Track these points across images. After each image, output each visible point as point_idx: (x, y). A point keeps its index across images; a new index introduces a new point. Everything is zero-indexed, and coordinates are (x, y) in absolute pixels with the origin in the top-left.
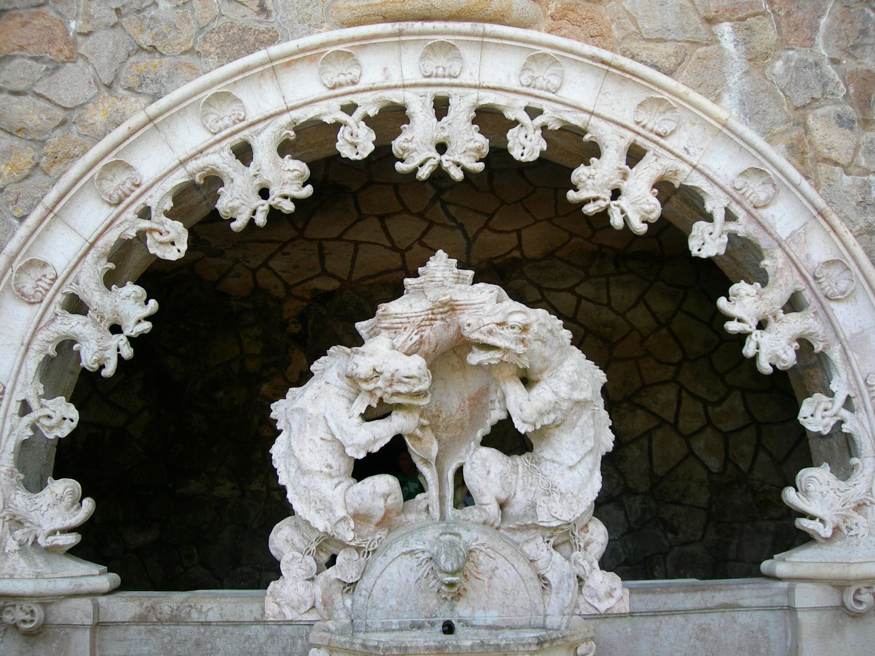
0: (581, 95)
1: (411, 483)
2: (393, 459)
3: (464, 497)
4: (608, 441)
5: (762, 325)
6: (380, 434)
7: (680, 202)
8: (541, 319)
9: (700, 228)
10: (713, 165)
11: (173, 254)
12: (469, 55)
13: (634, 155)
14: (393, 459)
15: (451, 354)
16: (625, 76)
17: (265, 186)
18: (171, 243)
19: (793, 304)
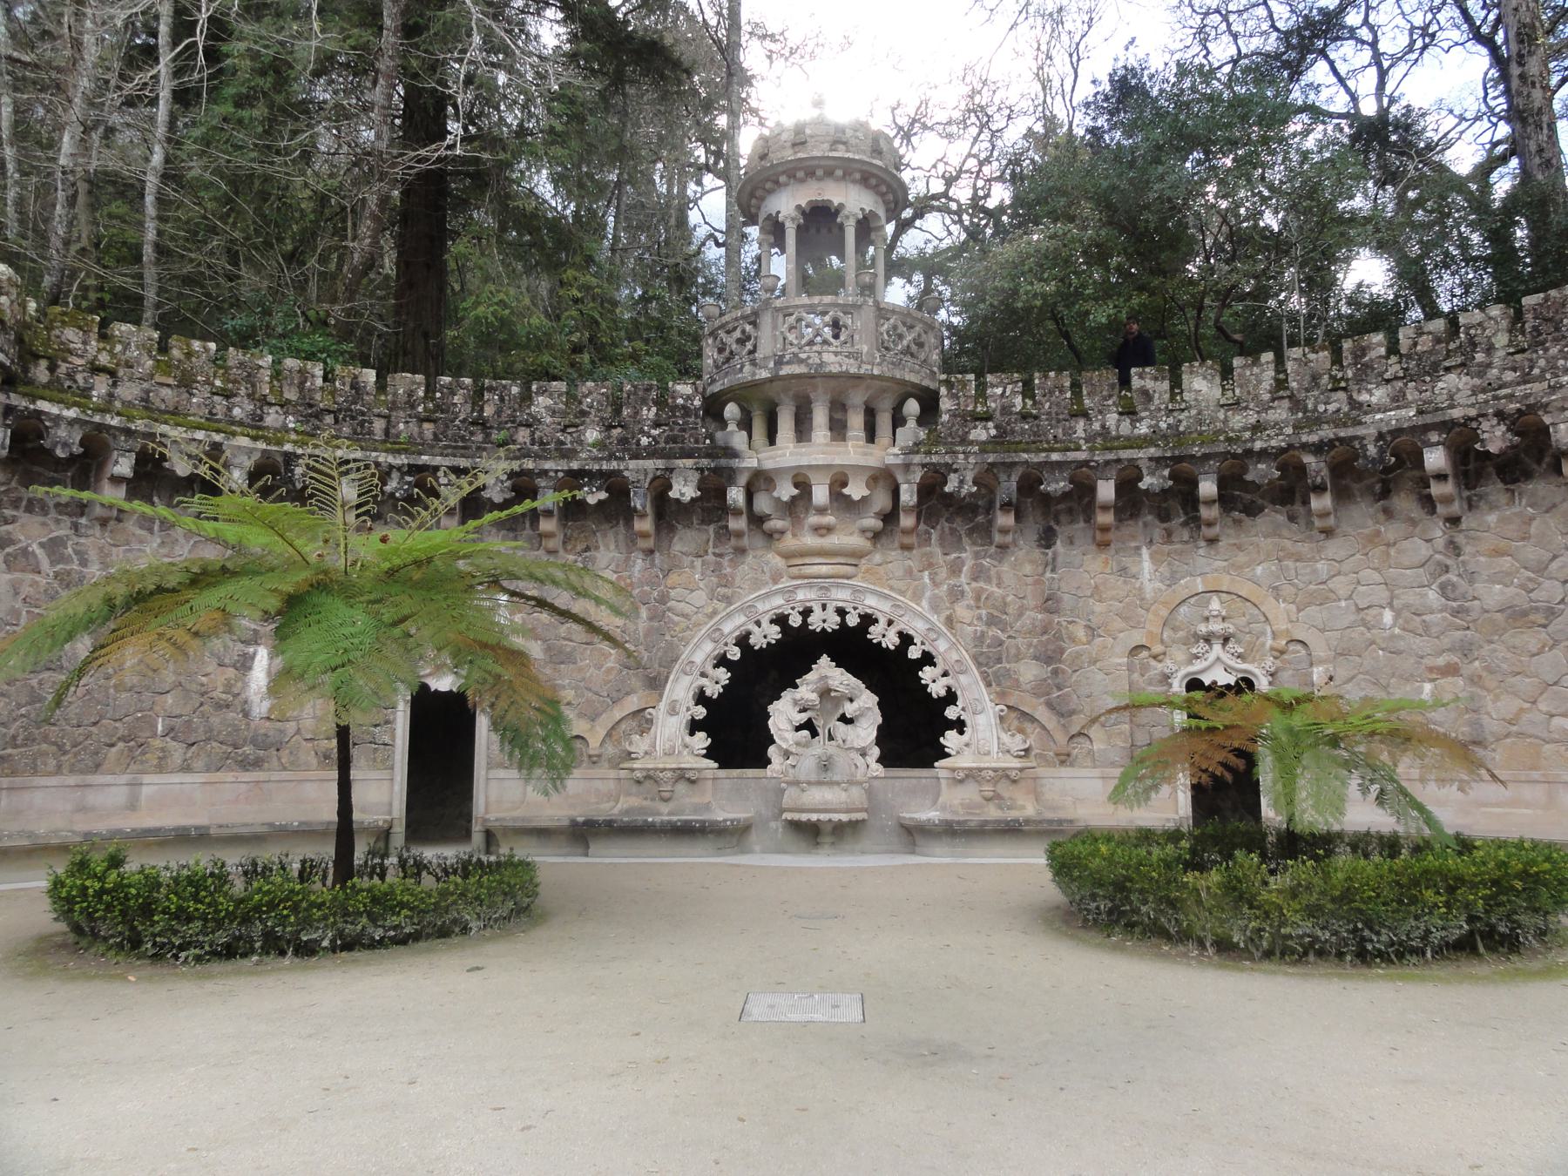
0: (871, 603)
1: (814, 734)
2: (809, 726)
3: (831, 738)
4: (880, 720)
5: (933, 681)
6: (804, 717)
9: (912, 648)
10: (916, 628)
11: (736, 658)
12: (834, 591)
13: (890, 623)
14: (809, 726)
15: (825, 693)
16: (887, 597)
18: (735, 654)
19: (945, 674)
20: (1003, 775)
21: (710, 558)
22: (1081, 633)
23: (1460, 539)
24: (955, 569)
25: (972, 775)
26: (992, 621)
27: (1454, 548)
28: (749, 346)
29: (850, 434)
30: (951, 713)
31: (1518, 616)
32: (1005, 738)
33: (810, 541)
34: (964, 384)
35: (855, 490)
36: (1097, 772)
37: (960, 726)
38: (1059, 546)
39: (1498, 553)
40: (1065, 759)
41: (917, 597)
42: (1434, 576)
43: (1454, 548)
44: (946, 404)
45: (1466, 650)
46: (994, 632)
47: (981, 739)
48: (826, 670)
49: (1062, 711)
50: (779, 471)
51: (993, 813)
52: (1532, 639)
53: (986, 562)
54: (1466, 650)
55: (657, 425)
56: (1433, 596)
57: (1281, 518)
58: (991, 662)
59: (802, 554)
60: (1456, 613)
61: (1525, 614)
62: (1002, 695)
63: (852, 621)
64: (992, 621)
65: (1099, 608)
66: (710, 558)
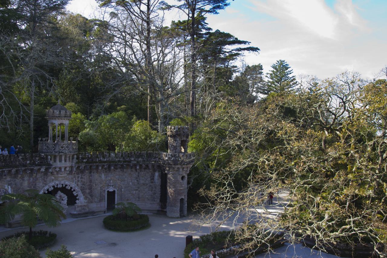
0: (67, 183)
7: (71, 188)
8: (65, 195)
17: (51, 189)
20: (85, 206)
21: (43, 178)
22: (94, 185)
23: (139, 175)
24: (78, 177)
25: (81, 206)
26: (83, 184)
27: (138, 176)
28: (54, 148)
29: (67, 161)
30: (77, 198)
31: (144, 184)
32: (85, 200)
33: (60, 176)
34: (83, 153)
35: (67, 169)
36: (96, 204)
38: (92, 173)
39: (142, 177)
40: (92, 202)
41: (73, 182)
42: (136, 179)
43: (138, 176)
44: (80, 156)
45: (139, 188)
46: (83, 186)
47: (81, 201)
48: (60, 193)
49: (91, 196)
50: (57, 167)
51: (83, 211)
53: (82, 176)
54: (139, 188)
55: (38, 160)
56: (136, 181)
57: (120, 170)
58: (83, 190)
60: (138, 183)
62: (84, 195)
63: (64, 186)
64: (83, 184)
65: (97, 182)
66: (43, 178)
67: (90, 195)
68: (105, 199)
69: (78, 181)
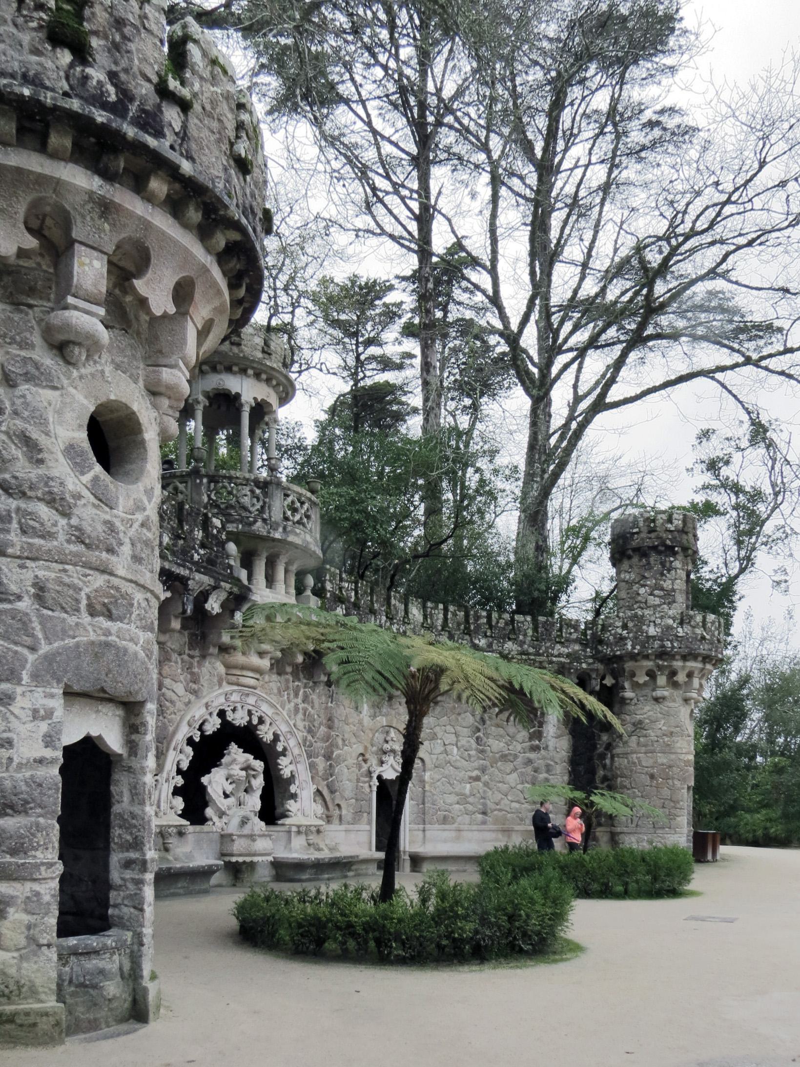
0: (266, 709)
22: (340, 742)
37: (294, 796)
45: (483, 770)
52: (509, 767)
56: (473, 742)
59: (243, 668)
61: (506, 756)
66: (185, 657)
67: (328, 786)
68: (369, 813)
69: (297, 710)
